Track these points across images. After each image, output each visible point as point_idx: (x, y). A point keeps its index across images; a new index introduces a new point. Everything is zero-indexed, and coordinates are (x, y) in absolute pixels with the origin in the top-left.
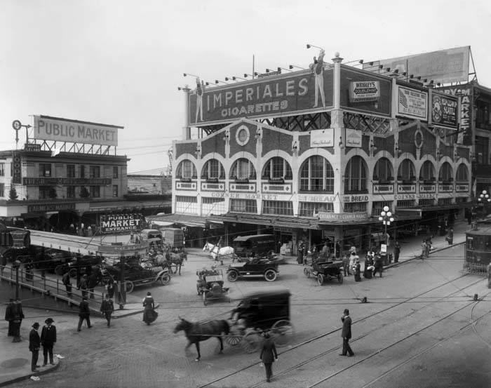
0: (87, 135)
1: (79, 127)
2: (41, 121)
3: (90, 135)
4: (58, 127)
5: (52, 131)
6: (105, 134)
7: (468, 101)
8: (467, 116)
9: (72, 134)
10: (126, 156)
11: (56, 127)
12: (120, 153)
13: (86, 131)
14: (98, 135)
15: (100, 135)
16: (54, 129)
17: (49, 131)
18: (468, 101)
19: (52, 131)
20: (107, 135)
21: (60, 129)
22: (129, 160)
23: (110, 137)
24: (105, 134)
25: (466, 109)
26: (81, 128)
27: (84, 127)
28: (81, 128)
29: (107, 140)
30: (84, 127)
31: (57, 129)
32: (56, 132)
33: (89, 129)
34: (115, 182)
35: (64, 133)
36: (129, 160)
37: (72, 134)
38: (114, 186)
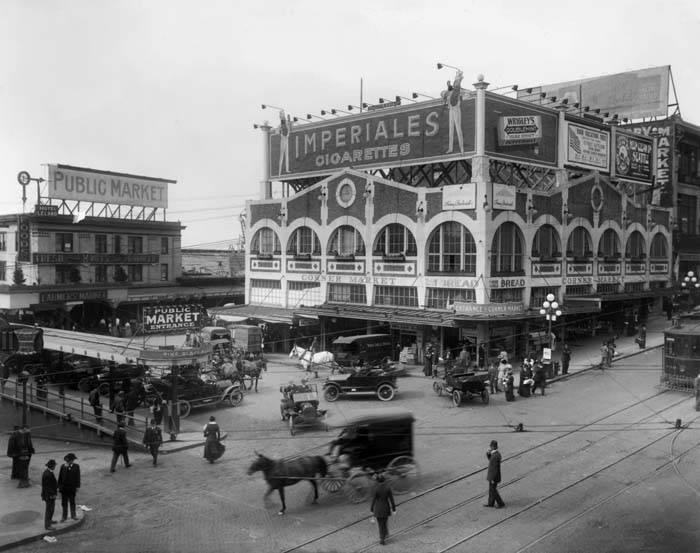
0: (124, 192)
1: (113, 182)
2: (59, 173)
3: (128, 193)
4: (83, 181)
5: (75, 187)
6: (149, 191)
9: (102, 191)
11: (80, 181)
13: (122, 186)
14: (140, 192)
15: (143, 192)
16: (77, 183)
17: (70, 187)
19: (75, 187)
20: (152, 192)
21: (85, 184)
23: (156, 196)
24: (149, 191)
26: (116, 183)
27: (119, 181)
28: (116, 183)
29: (153, 199)
30: (119, 181)
31: (82, 184)
32: (80, 188)
33: (126, 184)
35: (91, 189)
37: (102, 191)
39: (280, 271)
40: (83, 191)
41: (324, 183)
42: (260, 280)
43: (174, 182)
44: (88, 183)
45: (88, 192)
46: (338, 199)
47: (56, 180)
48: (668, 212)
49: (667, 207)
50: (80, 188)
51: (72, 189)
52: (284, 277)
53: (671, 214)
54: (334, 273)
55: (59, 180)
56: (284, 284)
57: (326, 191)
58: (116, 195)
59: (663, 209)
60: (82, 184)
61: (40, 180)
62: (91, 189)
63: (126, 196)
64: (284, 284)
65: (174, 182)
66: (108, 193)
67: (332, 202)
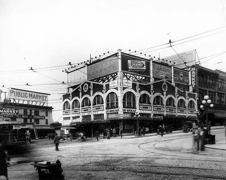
0: (33, 97)
1: (30, 94)
2: (12, 91)
4: (20, 93)
6: (42, 97)
7: (194, 73)
8: (194, 80)
9: (26, 97)
10: (52, 107)
12: (49, 105)
13: (33, 95)
14: (39, 97)
16: (18, 94)
17: (16, 95)
18: (194, 73)
20: (43, 98)
21: (21, 94)
22: (53, 108)
23: (44, 99)
24: (42, 97)
25: (194, 77)
26: (31, 94)
27: (32, 94)
28: (31, 94)
29: (43, 100)
30: (32, 94)
31: (20, 94)
34: (46, 118)
35: (23, 96)
36: (53, 108)
37: (26, 97)
38: (46, 119)
39: (70, 114)
40: (20, 96)
41: (80, 86)
42: (66, 118)
43: (50, 95)
44: (22, 94)
45: (22, 97)
46: (84, 90)
47: (11, 93)
48: (195, 94)
49: (195, 92)
50: (19, 95)
51: (16, 96)
52: (71, 116)
53: (196, 95)
54: (83, 113)
55: (12, 93)
56: (71, 118)
57: (81, 88)
58: (31, 98)
59: (193, 93)
60: (20, 94)
61: (5, 93)
62: (23, 96)
63: (34, 98)
64: (71, 118)
65: (50, 95)
66: (28, 97)
67: (82, 91)
